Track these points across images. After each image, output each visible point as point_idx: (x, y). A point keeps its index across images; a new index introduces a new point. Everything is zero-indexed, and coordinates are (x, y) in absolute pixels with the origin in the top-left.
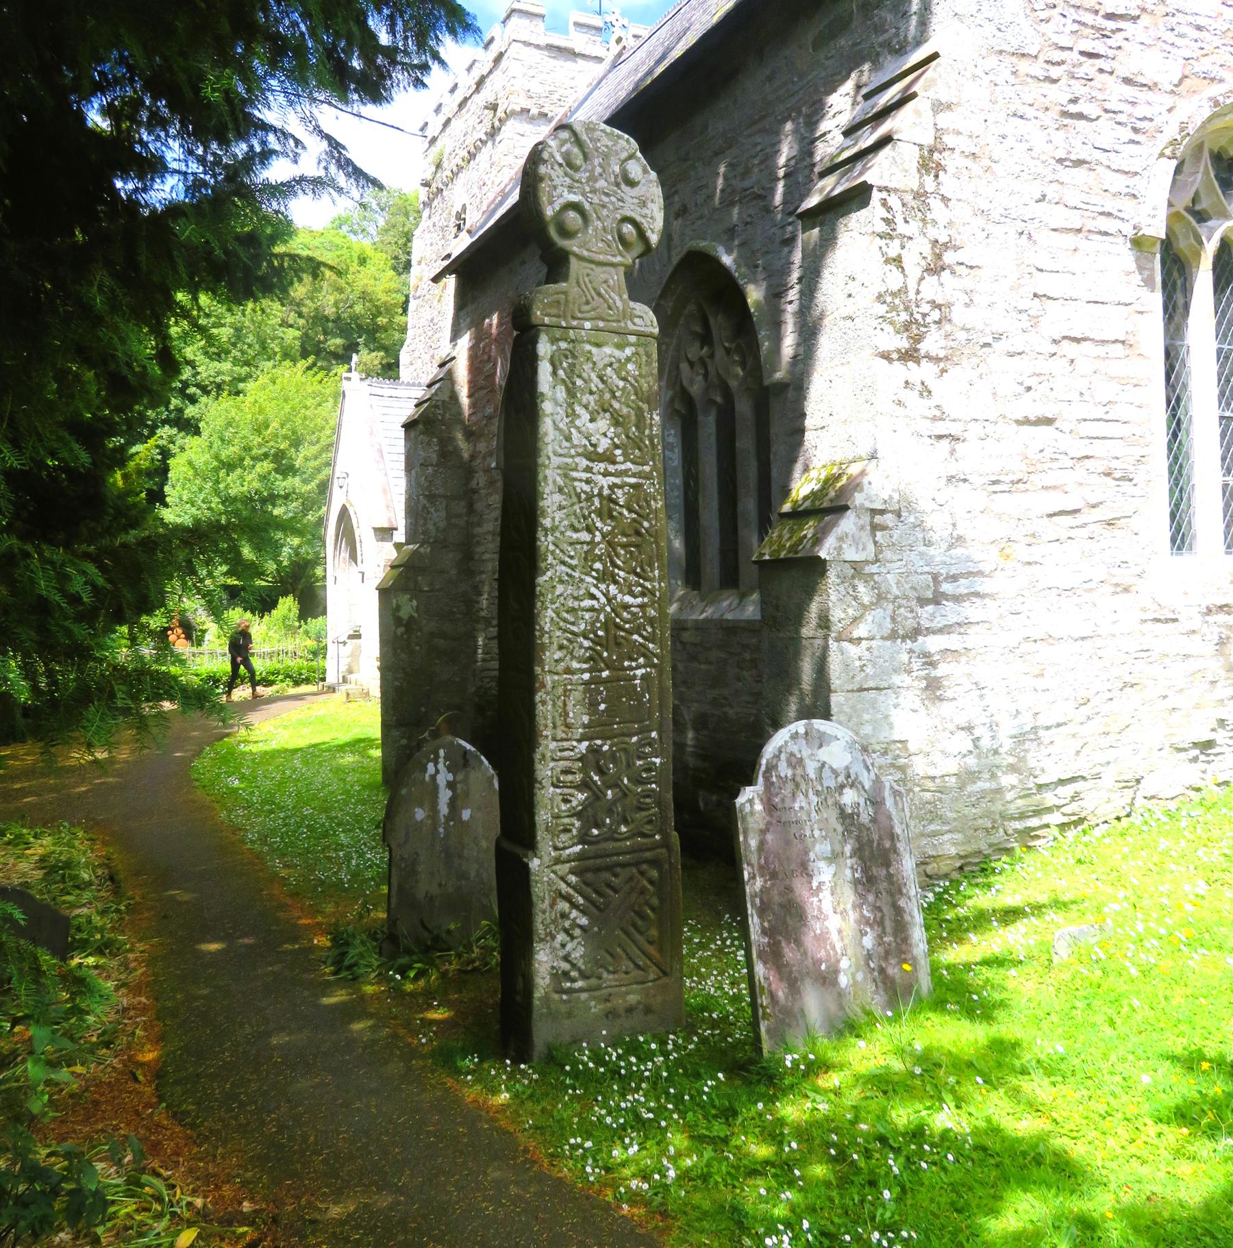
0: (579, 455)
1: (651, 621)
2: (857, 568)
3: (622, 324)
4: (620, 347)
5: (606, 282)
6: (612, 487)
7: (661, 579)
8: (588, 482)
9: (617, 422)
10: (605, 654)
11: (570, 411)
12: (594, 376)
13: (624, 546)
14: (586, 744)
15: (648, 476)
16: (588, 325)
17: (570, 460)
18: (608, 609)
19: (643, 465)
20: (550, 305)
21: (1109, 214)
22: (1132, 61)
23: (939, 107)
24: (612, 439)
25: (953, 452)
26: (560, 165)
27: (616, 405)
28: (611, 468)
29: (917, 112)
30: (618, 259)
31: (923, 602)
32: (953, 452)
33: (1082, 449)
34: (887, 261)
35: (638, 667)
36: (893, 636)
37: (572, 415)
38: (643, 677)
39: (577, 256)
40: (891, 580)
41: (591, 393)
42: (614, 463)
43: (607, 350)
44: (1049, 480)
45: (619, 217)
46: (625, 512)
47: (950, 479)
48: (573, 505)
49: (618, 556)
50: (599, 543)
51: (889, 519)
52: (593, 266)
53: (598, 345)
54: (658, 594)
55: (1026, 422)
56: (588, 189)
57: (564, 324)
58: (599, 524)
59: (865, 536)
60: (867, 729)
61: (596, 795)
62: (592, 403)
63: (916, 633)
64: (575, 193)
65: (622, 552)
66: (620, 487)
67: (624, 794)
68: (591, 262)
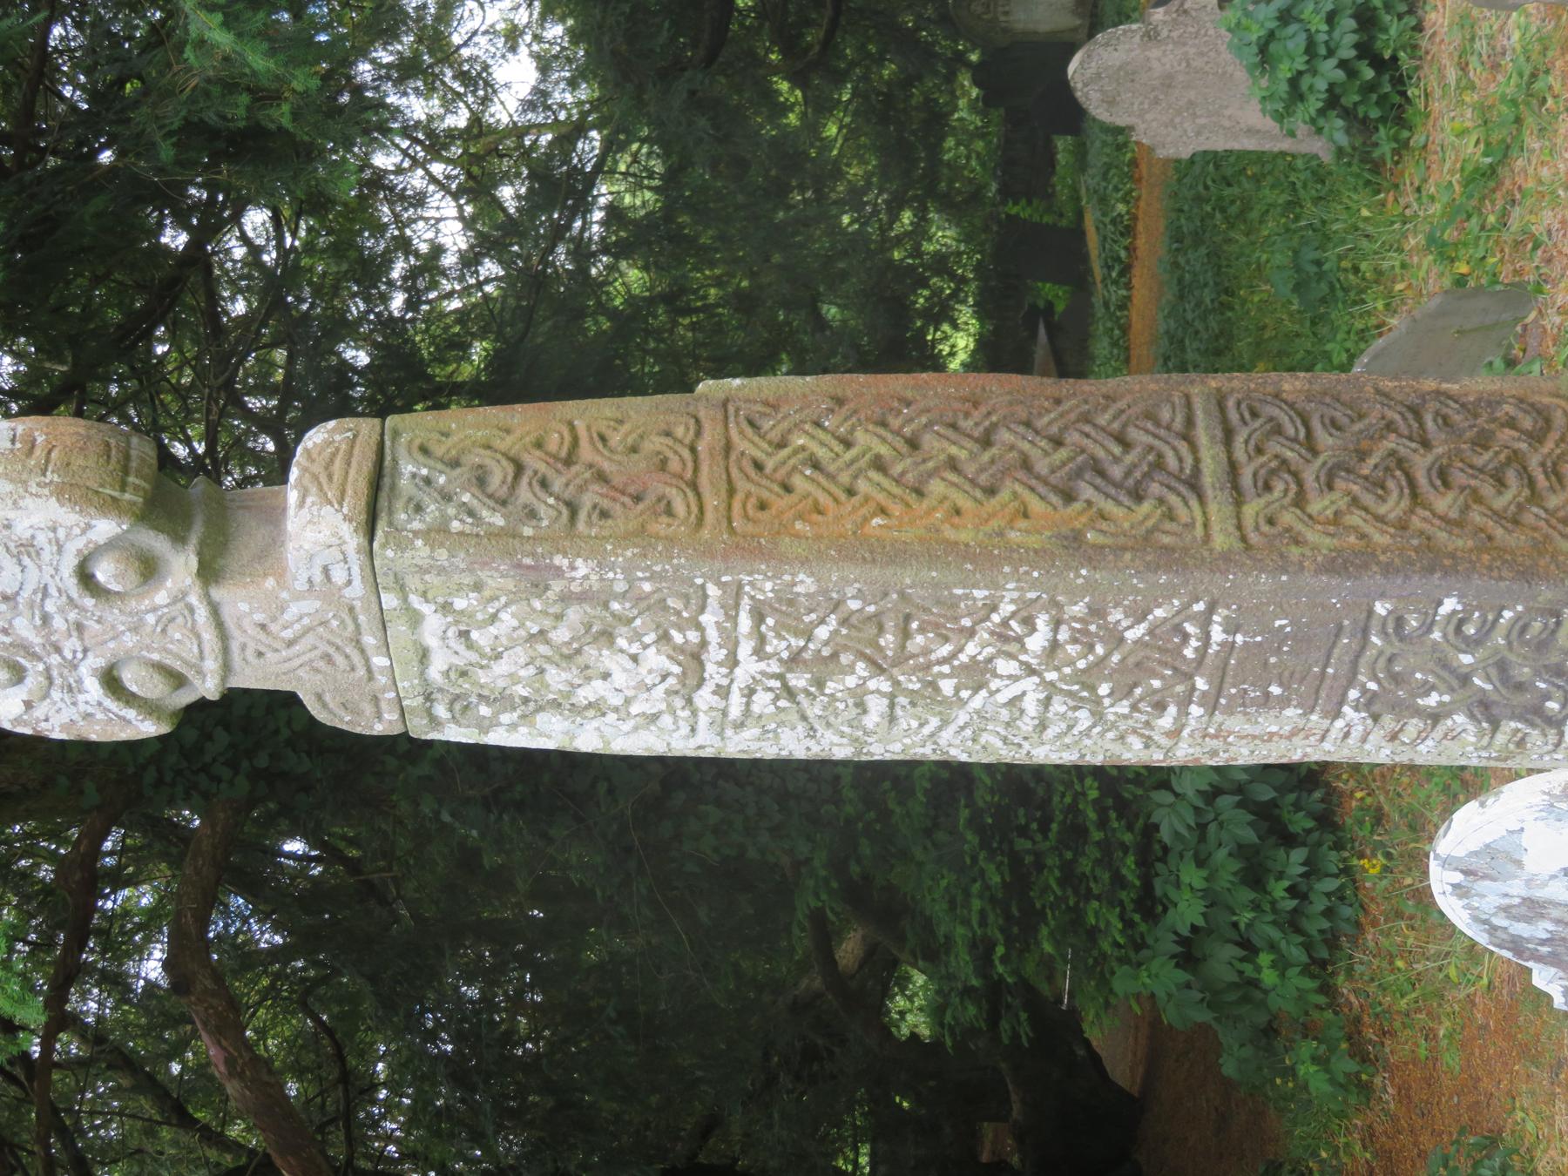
0: (689, 701)
1: (1097, 612)
3: (358, 604)
4: (416, 619)
5: (263, 627)
6: (759, 653)
7: (996, 586)
8: (750, 693)
10: (1156, 684)
11: (591, 713)
12: (501, 668)
13: (906, 635)
14: (1346, 709)
15: (735, 594)
16: (379, 661)
17: (703, 720)
18: (1051, 676)
19: (705, 596)
20: (357, 712)
24: (645, 647)
26: (28, 705)
27: (561, 635)
28: (715, 654)
30: (193, 599)
35: (1206, 638)
38: (1231, 628)
39: (224, 679)
41: (541, 671)
42: (704, 644)
43: (432, 641)
45: (89, 602)
46: (822, 633)
48: (804, 718)
49: (926, 651)
50: (896, 683)
52: (235, 647)
53: (424, 655)
54: (1032, 595)
56: (55, 659)
57: (392, 695)
58: (851, 681)
62: (565, 676)
64: (80, 681)
65: (919, 639)
66: (762, 640)
68: (226, 650)
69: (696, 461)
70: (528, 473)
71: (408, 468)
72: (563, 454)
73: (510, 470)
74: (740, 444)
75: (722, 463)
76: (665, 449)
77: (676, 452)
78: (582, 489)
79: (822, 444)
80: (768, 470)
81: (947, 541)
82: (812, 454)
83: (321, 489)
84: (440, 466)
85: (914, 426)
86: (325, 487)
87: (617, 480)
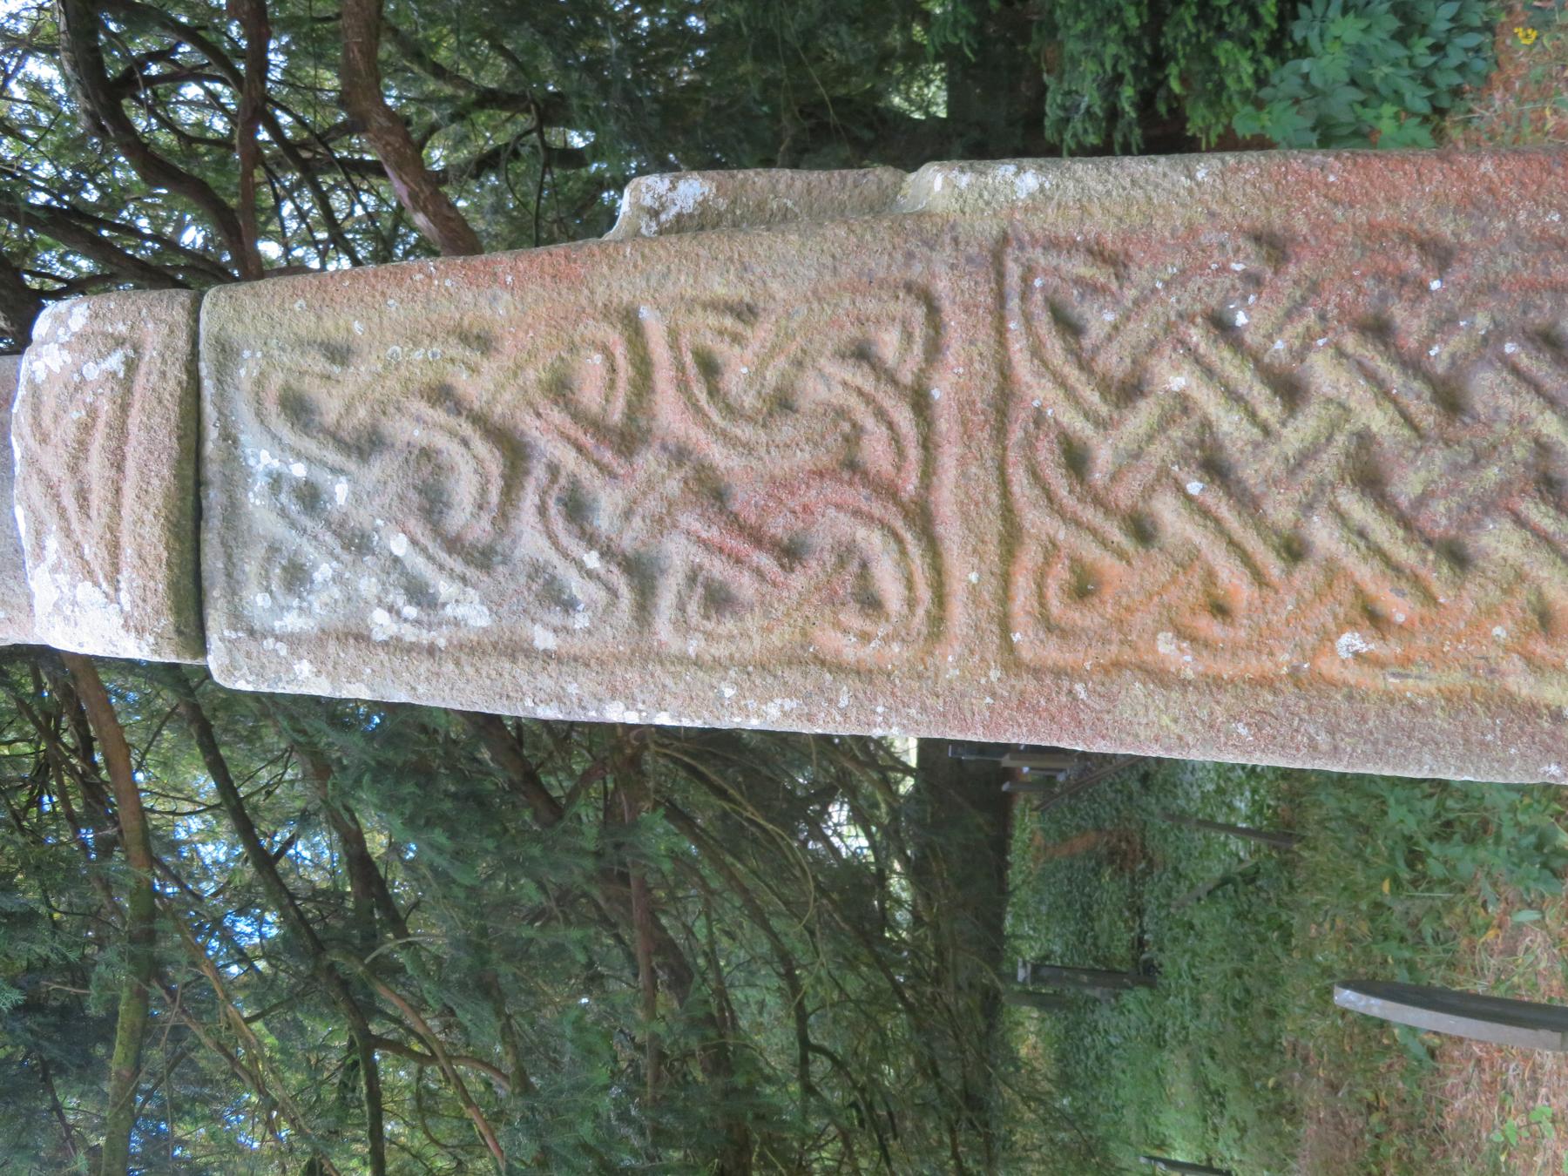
69: (928, 445)
70: (539, 472)
71: (262, 458)
72: (616, 416)
73: (494, 465)
74: (1038, 392)
75: (989, 451)
76: (853, 401)
77: (881, 414)
78: (661, 524)
79: (1234, 397)
80: (1098, 477)
81: (1509, 702)
82: (1206, 425)
83: (68, 533)
84: (333, 457)
85: (1458, 342)
86: (75, 525)
87: (745, 500)
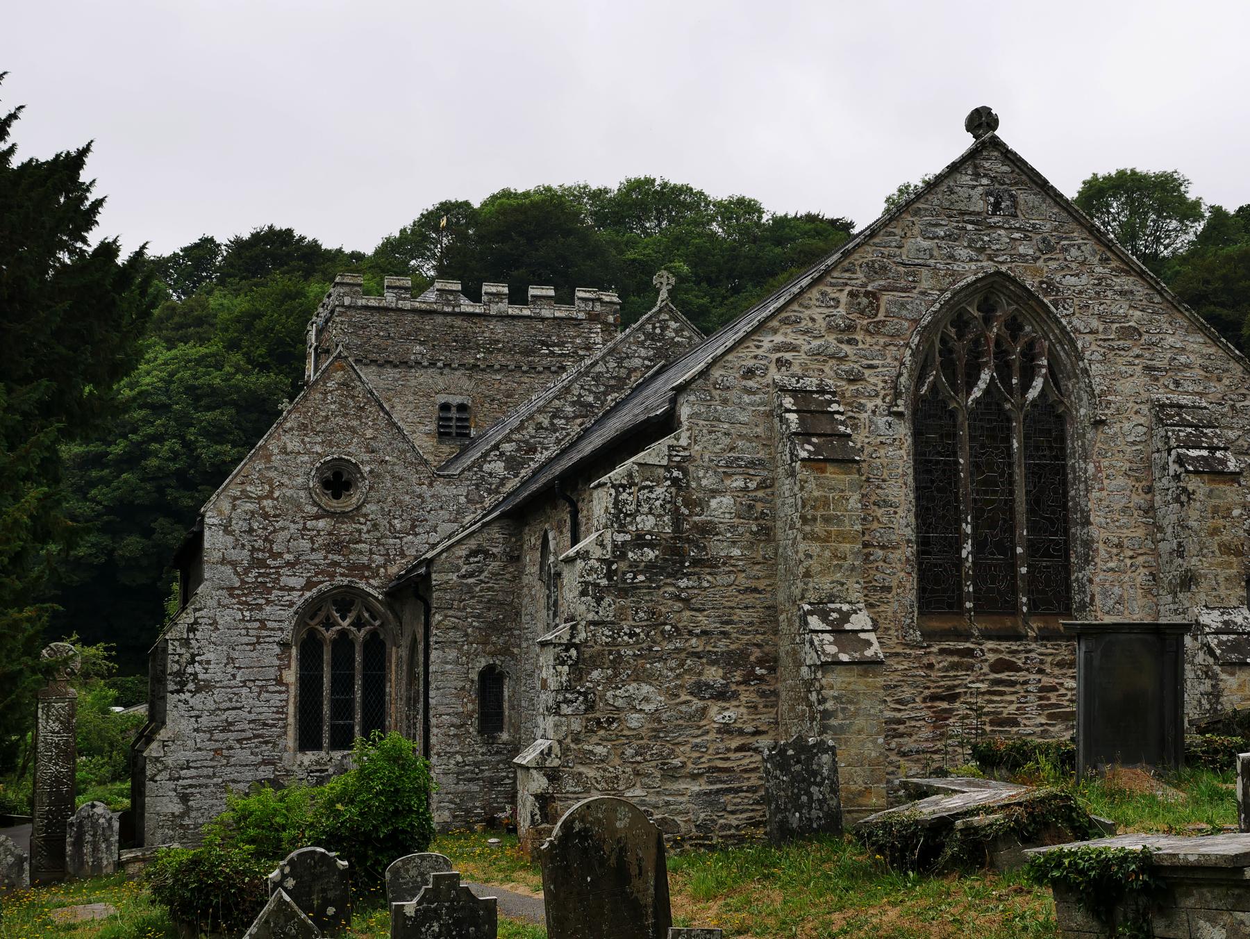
2: (157, 759)
9: (61, 722)
21: (270, 636)
22: (284, 580)
23: (196, 610)
25: (197, 721)
29: (187, 614)
31: (182, 769)
32: (197, 721)
33: (253, 716)
34: (173, 662)
36: (169, 780)
37: (47, 722)
40: (169, 761)
44: (236, 728)
47: (195, 730)
51: (170, 743)
55: (228, 709)
59: (160, 749)
60: (158, 808)
61: (50, 821)
63: (178, 779)
67: (59, 821)
